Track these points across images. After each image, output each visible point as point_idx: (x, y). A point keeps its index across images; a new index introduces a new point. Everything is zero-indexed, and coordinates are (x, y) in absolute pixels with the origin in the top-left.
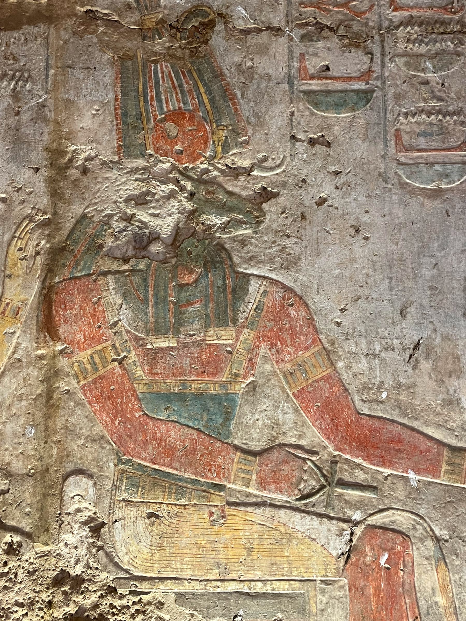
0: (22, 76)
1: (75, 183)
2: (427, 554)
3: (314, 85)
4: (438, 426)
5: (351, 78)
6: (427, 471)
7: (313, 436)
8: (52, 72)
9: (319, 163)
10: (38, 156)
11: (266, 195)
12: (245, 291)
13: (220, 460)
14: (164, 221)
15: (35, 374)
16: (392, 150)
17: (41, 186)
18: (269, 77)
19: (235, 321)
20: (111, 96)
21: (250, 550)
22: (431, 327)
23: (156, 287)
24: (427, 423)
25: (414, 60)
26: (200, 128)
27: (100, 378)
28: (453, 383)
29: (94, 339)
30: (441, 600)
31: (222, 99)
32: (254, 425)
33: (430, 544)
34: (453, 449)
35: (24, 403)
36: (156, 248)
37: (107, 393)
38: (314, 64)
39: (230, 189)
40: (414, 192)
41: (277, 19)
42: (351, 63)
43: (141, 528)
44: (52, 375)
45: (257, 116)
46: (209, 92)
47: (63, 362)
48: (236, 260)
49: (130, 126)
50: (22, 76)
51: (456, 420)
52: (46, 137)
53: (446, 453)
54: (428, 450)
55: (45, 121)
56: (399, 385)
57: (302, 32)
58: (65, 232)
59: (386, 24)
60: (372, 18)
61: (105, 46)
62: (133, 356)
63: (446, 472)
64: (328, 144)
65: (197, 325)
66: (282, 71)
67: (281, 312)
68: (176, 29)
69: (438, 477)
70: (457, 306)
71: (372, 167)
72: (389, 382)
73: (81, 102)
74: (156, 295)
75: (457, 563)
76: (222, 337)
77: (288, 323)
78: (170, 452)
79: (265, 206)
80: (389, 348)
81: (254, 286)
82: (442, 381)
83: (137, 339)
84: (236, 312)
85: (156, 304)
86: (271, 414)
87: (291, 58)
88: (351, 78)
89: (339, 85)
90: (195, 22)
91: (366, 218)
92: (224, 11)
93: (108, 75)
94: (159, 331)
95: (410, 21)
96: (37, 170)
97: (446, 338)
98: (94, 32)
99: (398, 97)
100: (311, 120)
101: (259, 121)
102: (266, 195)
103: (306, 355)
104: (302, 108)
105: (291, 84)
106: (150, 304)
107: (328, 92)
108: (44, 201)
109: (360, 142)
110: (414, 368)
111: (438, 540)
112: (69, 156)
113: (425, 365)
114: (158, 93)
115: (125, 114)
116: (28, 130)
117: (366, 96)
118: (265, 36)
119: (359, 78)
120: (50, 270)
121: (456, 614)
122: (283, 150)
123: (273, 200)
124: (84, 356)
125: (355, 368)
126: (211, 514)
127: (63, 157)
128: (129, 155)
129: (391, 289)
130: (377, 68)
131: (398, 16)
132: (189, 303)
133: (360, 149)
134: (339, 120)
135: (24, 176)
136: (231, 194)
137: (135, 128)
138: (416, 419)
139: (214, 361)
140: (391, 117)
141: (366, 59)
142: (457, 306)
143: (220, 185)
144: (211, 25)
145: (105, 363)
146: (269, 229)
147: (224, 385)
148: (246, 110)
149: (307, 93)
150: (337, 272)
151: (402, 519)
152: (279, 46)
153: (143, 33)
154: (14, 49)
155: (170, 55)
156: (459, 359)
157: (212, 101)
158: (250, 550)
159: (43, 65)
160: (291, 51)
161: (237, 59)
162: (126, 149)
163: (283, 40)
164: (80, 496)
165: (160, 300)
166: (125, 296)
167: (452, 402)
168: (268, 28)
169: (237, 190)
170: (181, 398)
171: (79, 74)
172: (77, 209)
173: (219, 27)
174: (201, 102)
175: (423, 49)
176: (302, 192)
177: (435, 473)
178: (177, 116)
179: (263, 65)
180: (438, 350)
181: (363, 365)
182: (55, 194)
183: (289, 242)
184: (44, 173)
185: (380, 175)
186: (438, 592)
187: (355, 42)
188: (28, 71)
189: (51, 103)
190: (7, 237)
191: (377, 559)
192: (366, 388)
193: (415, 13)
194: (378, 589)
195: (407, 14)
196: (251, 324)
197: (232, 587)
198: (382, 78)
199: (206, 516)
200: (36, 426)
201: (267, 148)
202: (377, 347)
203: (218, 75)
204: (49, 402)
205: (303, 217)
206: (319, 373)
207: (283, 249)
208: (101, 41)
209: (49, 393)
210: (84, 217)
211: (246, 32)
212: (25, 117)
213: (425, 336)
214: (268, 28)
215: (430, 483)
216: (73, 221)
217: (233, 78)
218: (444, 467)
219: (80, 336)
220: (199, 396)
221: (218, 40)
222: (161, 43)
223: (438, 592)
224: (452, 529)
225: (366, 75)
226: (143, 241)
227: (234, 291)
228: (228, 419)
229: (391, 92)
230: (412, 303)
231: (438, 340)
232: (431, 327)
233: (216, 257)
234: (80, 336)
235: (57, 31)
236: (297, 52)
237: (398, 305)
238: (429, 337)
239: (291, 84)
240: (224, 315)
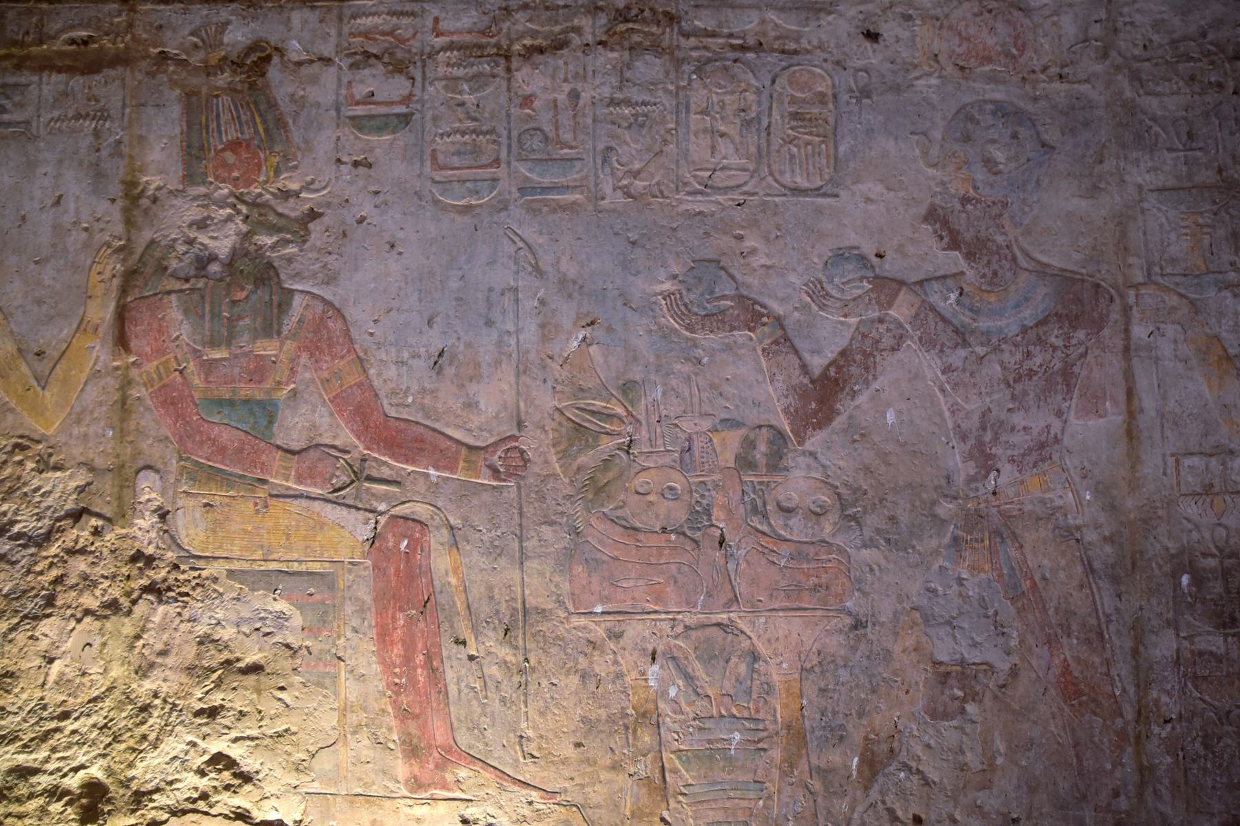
0: (103, 115)
1: (146, 212)
2: (442, 540)
3: (360, 110)
4: (458, 427)
5: (392, 103)
6: (446, 468)
7: (346, 437)
8: (128, 110)
9: (361, 183)
10: (116, 189)
11: (313, 215)
12: (289, 304)
13: (264, 457)
14: (222, 243)
15: (112, 383)
16: (428, 168)
18: (318, 105)
19: (279, 333)
20: (177, 130)
21: (288, 536)
22: (455, 335)
23: (212, 303)
24: (447, 425)
25: (452, 83)
26: (255, 155)
27: (164, 386)
28: (473, 388)
29: (161, 352)
30: (453, 580)
31: (275, 125)
32: (294, 427)
33: (445, 531)
34: (471, 448)
35: (104, 408)
36: (214, 268)
37: (171, 400)
38: (360, 91)
39: (280, 210)
40: (445, 208)
41: (327, 50)
42: (393, 88)
43: (198, 515)
44: (127, 383)
45: (306, 141)
46: (264, 121)
47: (134, 372)
48: (282, 276)
49: (194, 155)
50: (103, 115)
51: (476, 421)
52: (122, 171)
53: (464, 451)
54: (447, 449)
55: (121, 155)
56: (423, 390)
57: (350, 61)
58: (136, 256)
59: (428, 49)
60: (415, 45)
61: (174, 84)
62: (192, 367)
63: (463, 468)
64: (370, 166)
65: (246, 337)
66: (331, 98)
67: (319, 325)
68: (237, 65)
69: (455, 473)
70: (480, 315)
71: (408, 186)
72: (415, 387)
73: (152, 137)
74: (211, 311)
75: (468, 548)
76: (267, 348)
77: (328, 334)
78: (222, 450)
79: (311, 226)
80: (416, 356)
81: (297, 301)
82: (463, 385)
83: (195, 351)
84: (280, 325)
85: (212, 319)
86: (310, 418)
87: (339, 86)
88: (392, 103)
89: (382, 110)
90: (254, 57)
91: (401, 235)
92: (280, 45)
93: (175, 111)
94: (213, 343)
95: (450, 47)
96: (113, 201)
97: (469, 345)
98: (165, 72)
99: (435, 119)
100: (355, 143)
101: (308, 146)
102: (313, 215)
103: (342, 363)
104: (347, 132)
105: (338, 110)
106: (207, 319)
107: (372, 117)
108: (119, 228)
109: (398, 162)
110: (438, 373)
111: (452, 528)
112: (141, 188)
113: (450, 371)
114: (219, 125)
115: (189, 146)
117: (405, 119)
118: (316, 66)
119: (400, 103)
120: (124, 291)
121: (465, 591)
122: (329, 172)
123: (318, 221)
124: (151, 367)
125: (387, 375)
126: (256, 504)
127: (135, 188)
128: (193, 183)
129: (420, 301)
130: (417, 92)
131: (439, 41)
132: (240, 318)
135: (103, 206)
136: (280, 215)
137: (198, 158)
138: (437, 420)
139: (259, 370)
140: (428, 138)
141: (408, 84)
142: (480, 315)
143: (271, 208)
144: (268, 59)
145: (168, 372)
146: (313, 248)
147: (268, 392)
148: (296, 136)
149: (352, 118)
150: (373, 285)
151: (420, 510)
152: (329, 76)
153: (208, 70)
154: (95, 91)
155: (231, 90)
156: (479, 365)
157: (266, 130)
158: (288, 536)
159: (120, 104)
160: (339, 80)
161: (290, 90)
162: (190, 178)
163: (332, 70)
164: (149, 490)
165: (215, 315)
166: (186, 312)
167: (471, 405)
168: (320, 59)
169: (286, 212)
170: (231, 403)
171: (150, 111)
172: (148, 235)
173: (276, 59)
174: (256, 131)
175: (460, 72)
176: (345, 211)
177: (452, 469)
178: (234, 146)
179: (313, 93)
180: (461, 357)
181: (392, 371)
182: (129, 222)
183: (330, 259)
184: (120, 203)
185: (416, 193)
186: (450, 574)
187: (399, 68)
188: (108, 110)
189: (126, 139)
190: (89, 262)
191: (398, 544)
192: (394, 393)
193: (455, 38)
194: (397, 570)
195: (447, 39)
196: (293, 336)
197: (273, 566)
198: (422, 102)
199: (251, 505)
200: (113, 428)
201: (313, 173)
202: (406, 355)
203: (273, 105)
204: (124, 407)
205: (345, 235)
206: (352, 380)
207: (325, 266)
208: (170, 80)
209: (124, 401)
210: (153, 242)
211: (299, 64)
212: (104, 153)
213: (450, 344)
214: (320, 59)
215: (448, 479)
216: (144, 245)
217: (286, 107)
218: (462, 464)
219: (148, 349)
220: (247, 401)
221: (274, 72)
222: (223, 79)
223: (450, 574)
224: (465, 519)
225: (407, 100)
226: (203, 262)
227: (280, 305)
228: (271, 422)
229: (429, 115)
230: (439, 313)
231: (461, 348)
232: (455, 335)
233: (265, 274)
234: (148, 349)
235: (132, 72)
236: (345, 80)
237: (426, 315)
238: (453, 345)
239: (338, 110)
240: (270, 329)
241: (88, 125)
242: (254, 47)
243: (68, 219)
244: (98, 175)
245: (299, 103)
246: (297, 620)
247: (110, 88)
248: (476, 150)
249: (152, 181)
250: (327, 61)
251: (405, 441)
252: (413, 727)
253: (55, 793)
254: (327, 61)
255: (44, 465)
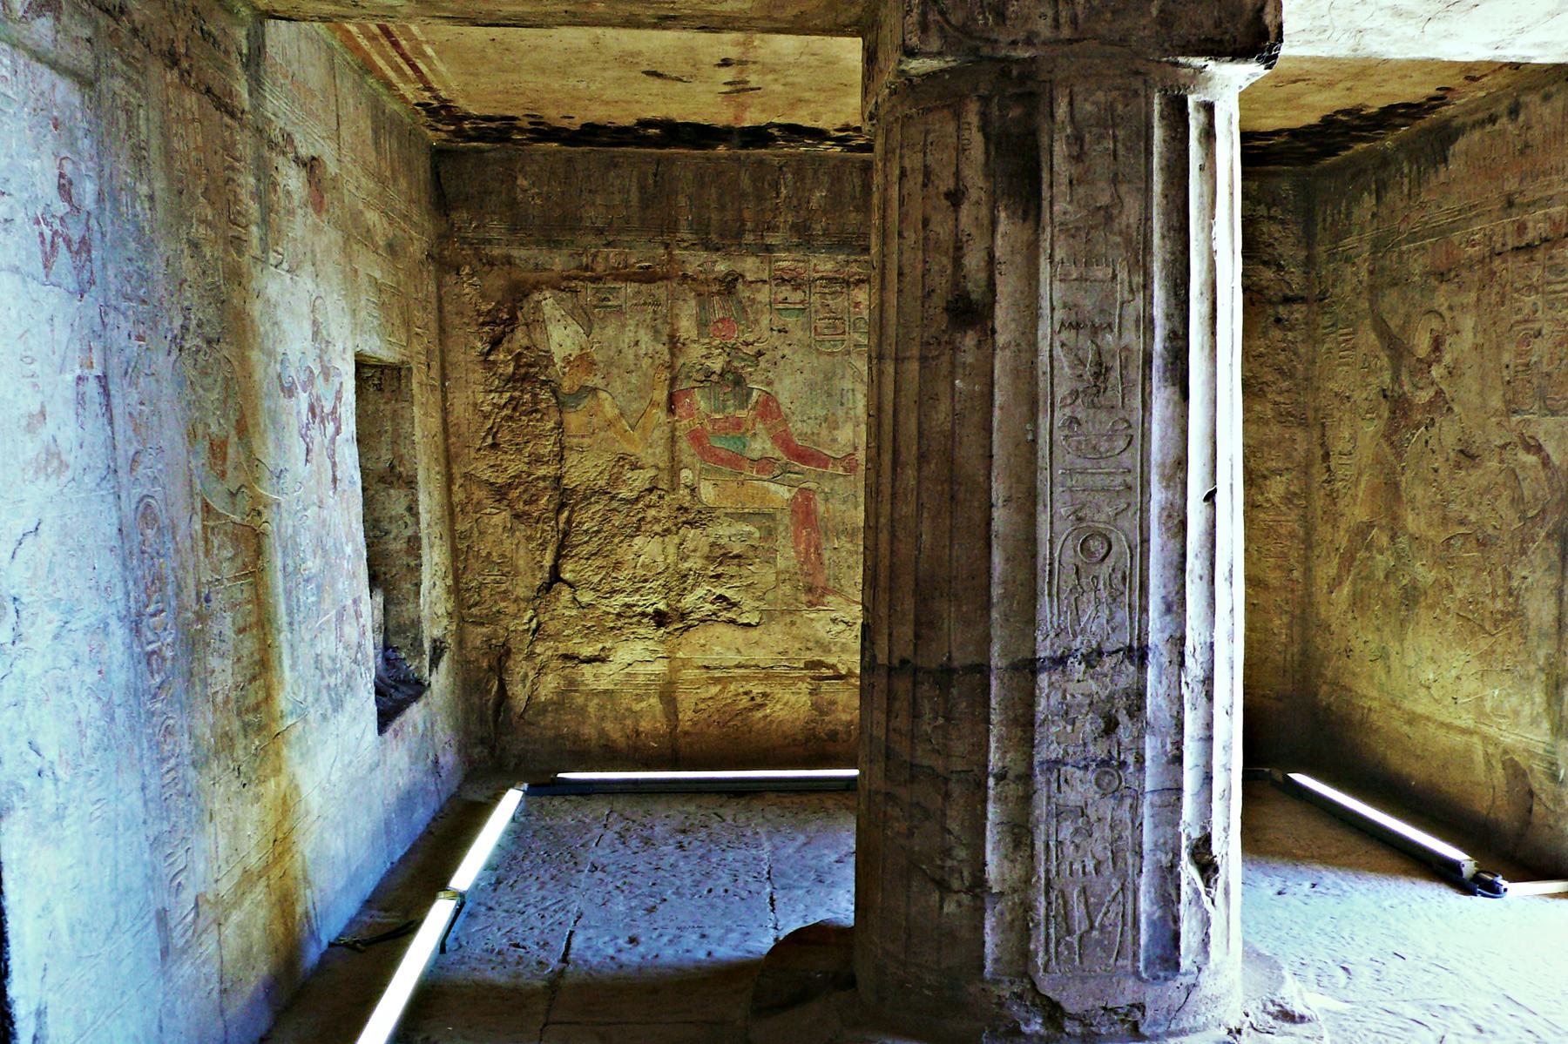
7: (778, 454)
10: (665, 339)
11: (760, 354)
14: (717, 365)
17: (666, 351)
29: (691, 415)
36: (714, 378)
37: (697, 437)
38: (780, 297)
40: (821, 353)
41: (765, 276)
44: (673, 430)
49: (702, 324)
60: (805, 276)
61: (692, 290)
67: (766, 404)
76: (742, 414)
77: (769, 408)
81: (755, 394)
93: (693, 303)
95: (822, 278)
102: (760, 354)
104: (775, 317)
116: (660, 327)
125: (797, 427)
131: (817, 275)
133: (800, 334)
134: (790, 321)
135: (659, 347)
151: (813, 485)
155: (719, 293)
172: (681, 361)
178: (722, 320)
182: (673, 354)
187: (797, 288)
204: (673, 440)
221: (740, 286)
225: (802, 302)
226: (709, 373)
233: (739, 381)
240: (742, 405)
241: (650, 309)
242: (728, 274)
243: (642, 352)
244: (656, 332)
245: (753, 301)
246: (757, 535)
247: (660, 291)
248: (835, 327)
249: (683, 335)
250: (764, 282)
251: (804, 456)
252: (809, 579)
253: (644, 614)
254: (764, 282)
255: (634, 467)
